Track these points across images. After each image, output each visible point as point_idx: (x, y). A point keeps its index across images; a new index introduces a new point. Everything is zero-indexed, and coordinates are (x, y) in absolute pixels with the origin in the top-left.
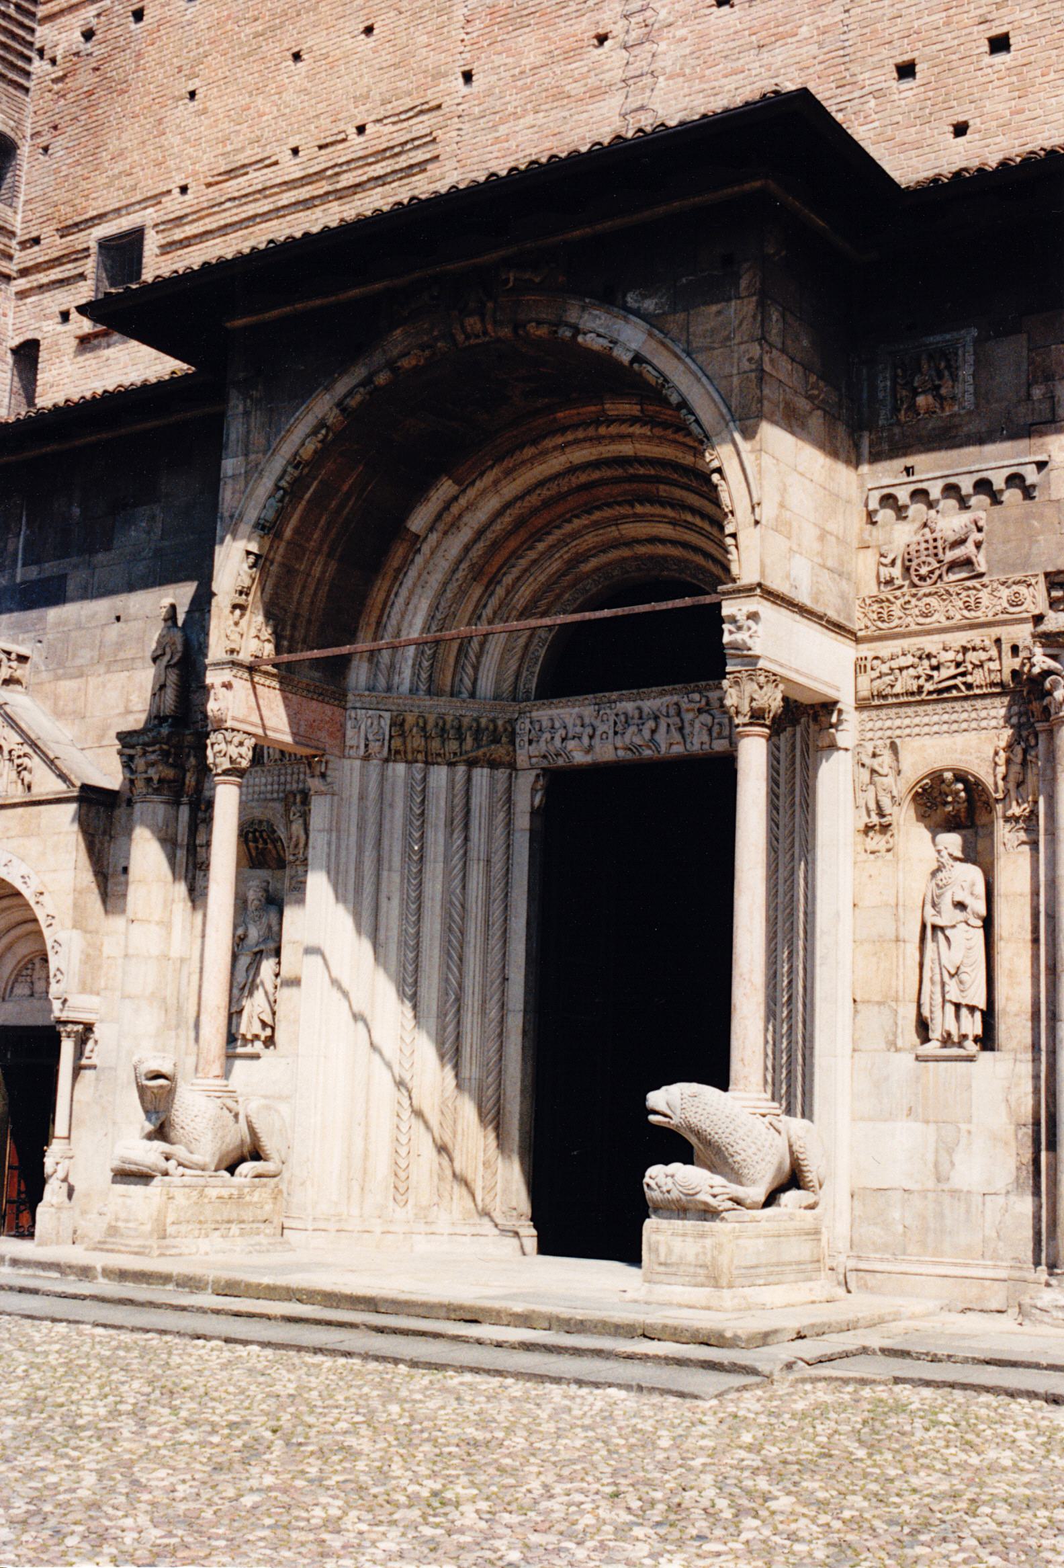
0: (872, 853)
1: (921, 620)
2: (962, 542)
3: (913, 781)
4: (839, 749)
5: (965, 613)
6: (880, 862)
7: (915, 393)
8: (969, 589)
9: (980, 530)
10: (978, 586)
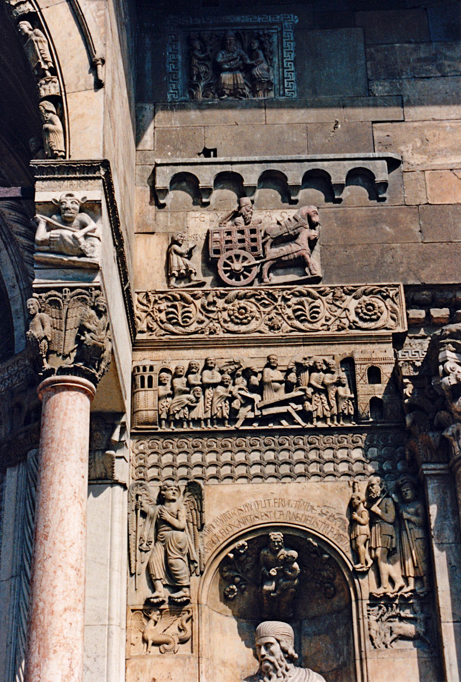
0: (156, 644)
1: (236, 328)
2: (292, 238)
3: (222, 541)
4: (117, 483)
5: (297, 323)
6: (169, 659)
7: (218, 69)
8: (301, 294)
9: (313, 225)
10: (314, 292)
